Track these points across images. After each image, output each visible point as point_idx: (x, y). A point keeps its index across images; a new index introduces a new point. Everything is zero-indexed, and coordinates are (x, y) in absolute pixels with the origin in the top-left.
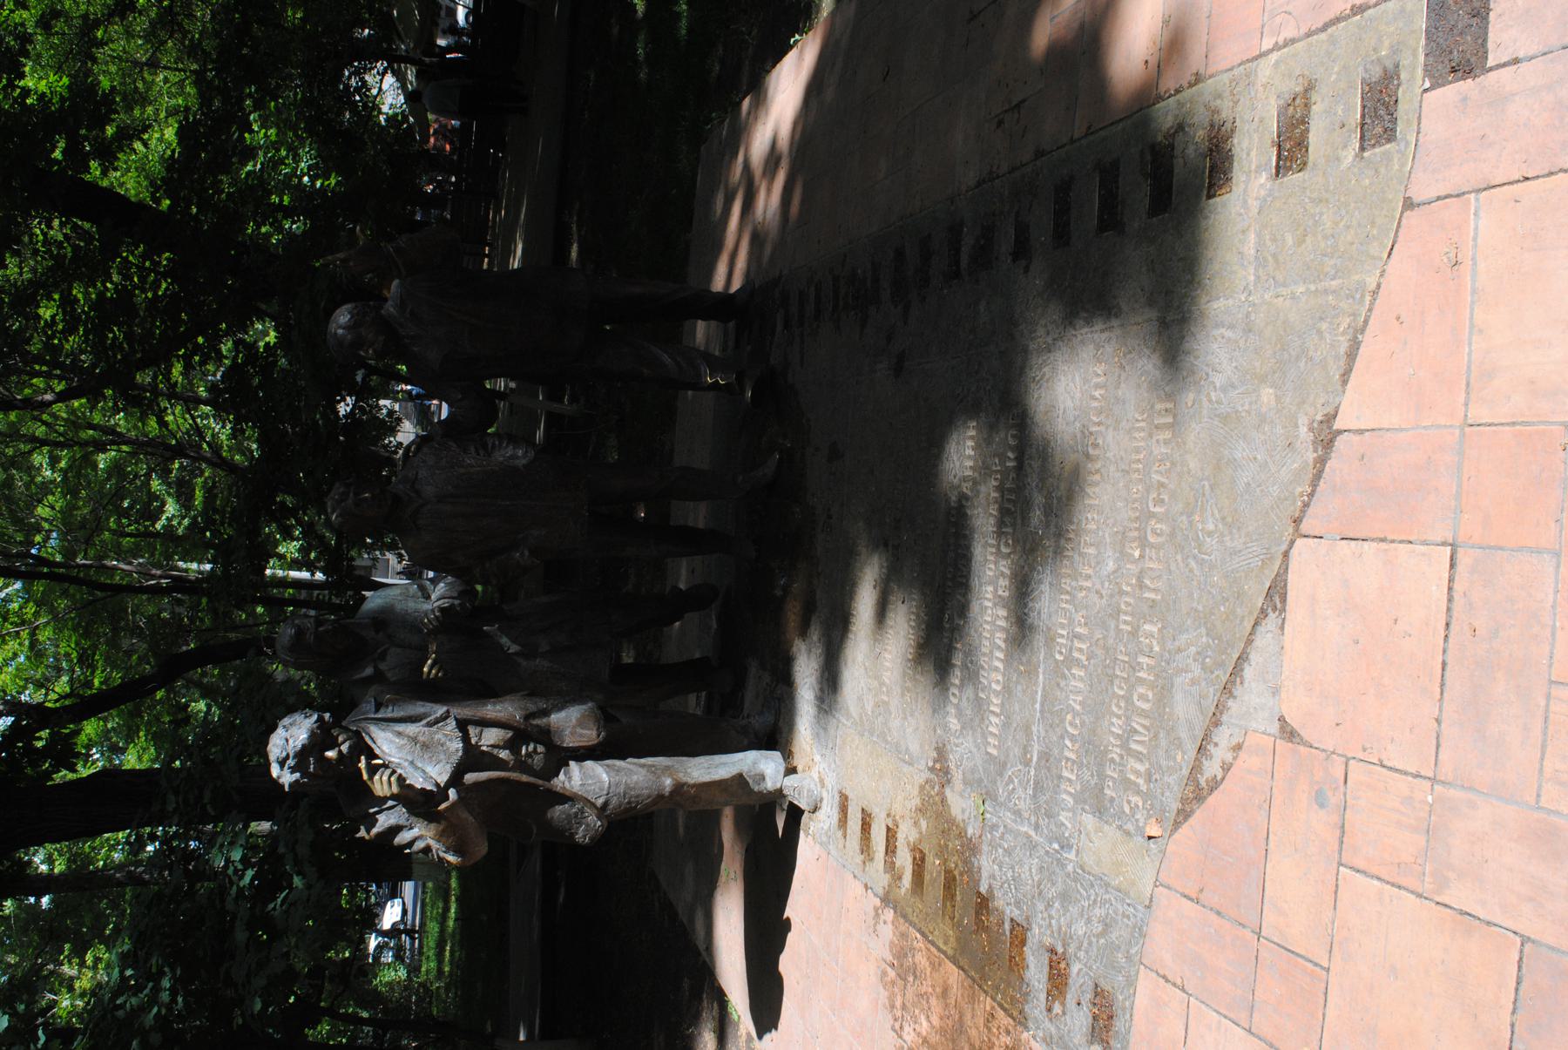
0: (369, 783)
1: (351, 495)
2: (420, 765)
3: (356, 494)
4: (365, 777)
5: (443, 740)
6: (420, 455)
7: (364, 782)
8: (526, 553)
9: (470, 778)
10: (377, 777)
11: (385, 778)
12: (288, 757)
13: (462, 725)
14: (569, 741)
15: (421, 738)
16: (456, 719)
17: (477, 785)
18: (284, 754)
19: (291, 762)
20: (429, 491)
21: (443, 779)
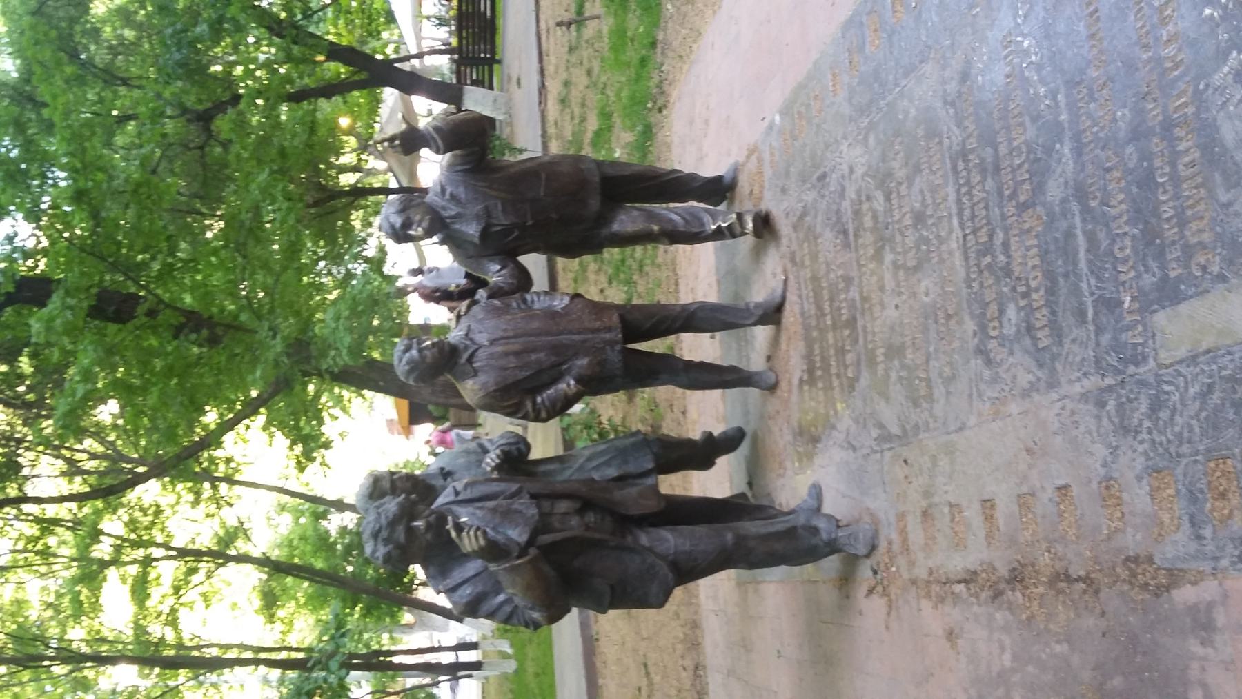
0: (457, 540)
1: (415, 346)
2: (501, 530)
3: (419, 343)
4: (453, 534)
5: (520, 507)
6: (471, 312)
7: (451, 541)
8: (572, 382)
9: (545, 539)
10: (464, 534)
11: (472, 533)
12: (380, 529)
13: (533, 496)
14: (634, 511)
15: (501, 509)
16: (529, 493)
17: (554, 544)
18: (377, 527)
19: (384, 534)
20: (482, 338)
21: (523, 538)
